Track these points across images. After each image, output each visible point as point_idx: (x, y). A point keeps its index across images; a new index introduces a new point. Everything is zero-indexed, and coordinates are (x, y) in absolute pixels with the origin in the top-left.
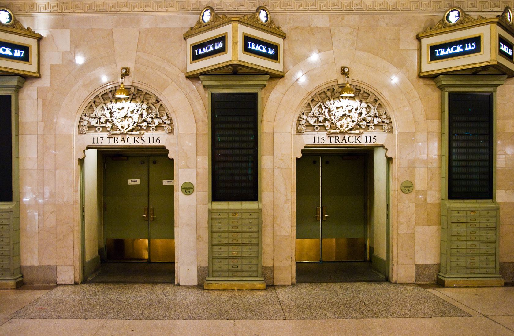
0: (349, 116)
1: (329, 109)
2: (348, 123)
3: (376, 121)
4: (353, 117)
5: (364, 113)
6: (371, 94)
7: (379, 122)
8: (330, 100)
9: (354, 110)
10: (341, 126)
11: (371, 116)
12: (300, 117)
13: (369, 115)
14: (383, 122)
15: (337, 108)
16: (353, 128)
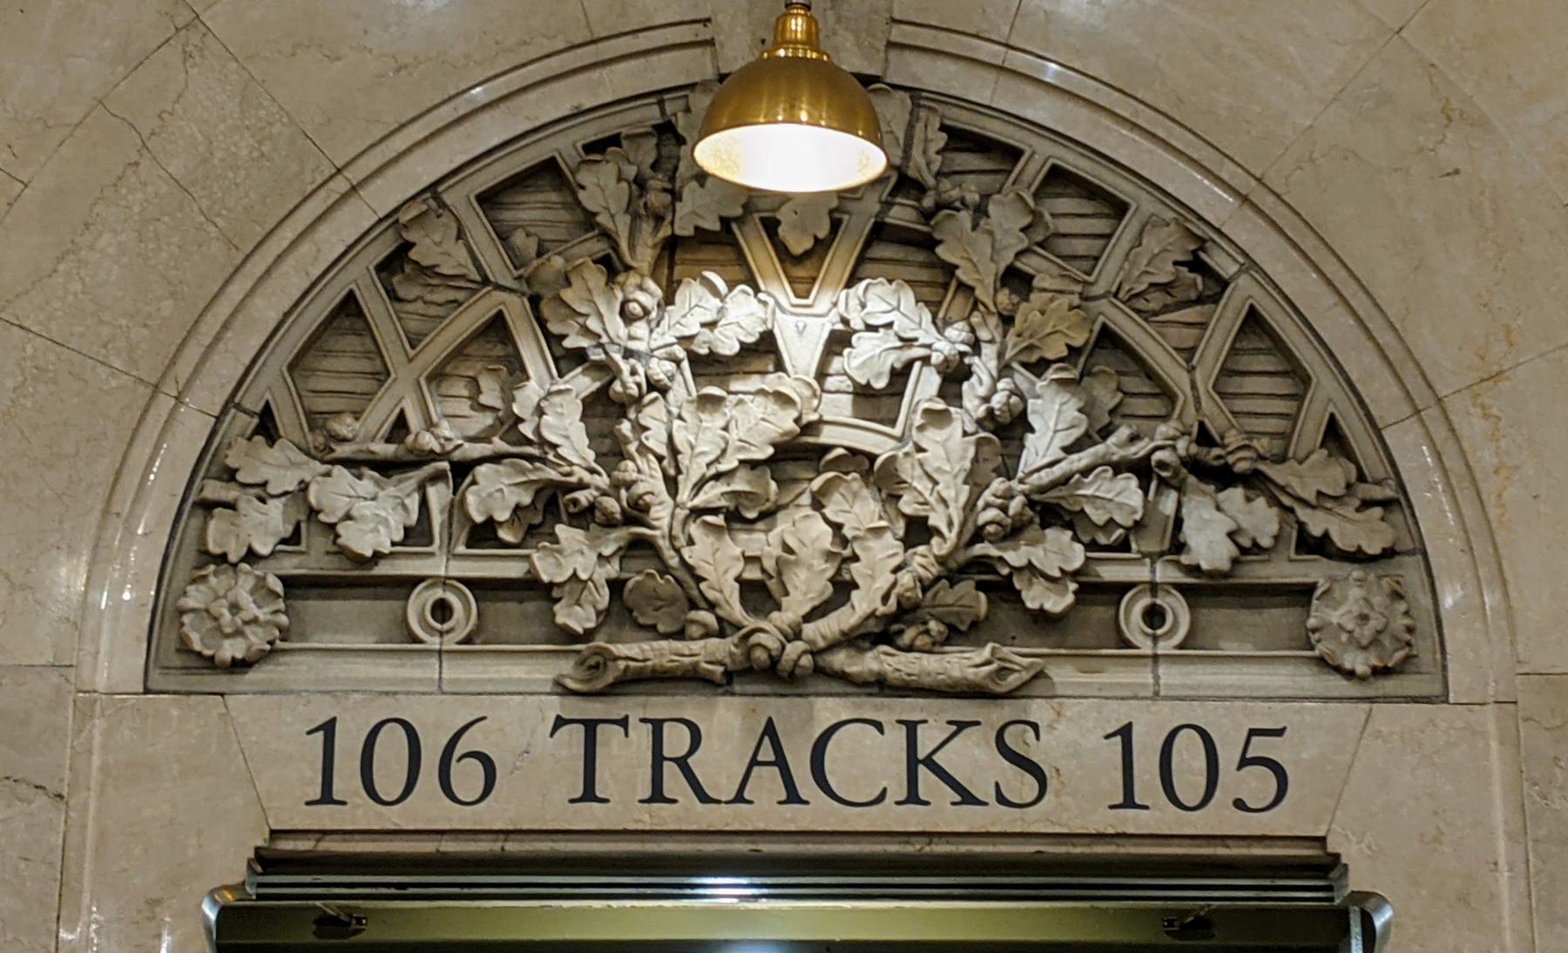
0: (858, 460)
1: (607, 370)
2: (843, 550)
3: (1210, 529)
4: (907, 470)
5: (1053, 418)
6: (1143, 204)
7: (1249, 551)
8: (613, 267)
9: (925, 387)
10: (759, 594)
11: (1142, 470)
12: (212, 463)
13: (1113, 446)
14: (1319, 546)
15: (708, 366)
16: (906, 612)
